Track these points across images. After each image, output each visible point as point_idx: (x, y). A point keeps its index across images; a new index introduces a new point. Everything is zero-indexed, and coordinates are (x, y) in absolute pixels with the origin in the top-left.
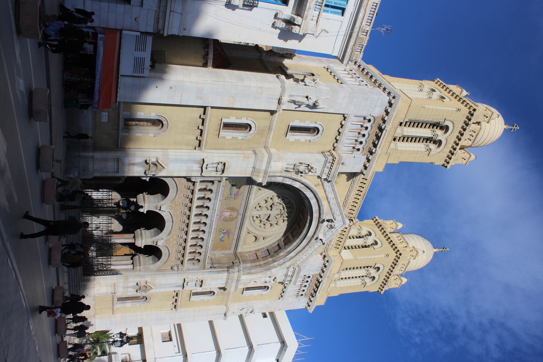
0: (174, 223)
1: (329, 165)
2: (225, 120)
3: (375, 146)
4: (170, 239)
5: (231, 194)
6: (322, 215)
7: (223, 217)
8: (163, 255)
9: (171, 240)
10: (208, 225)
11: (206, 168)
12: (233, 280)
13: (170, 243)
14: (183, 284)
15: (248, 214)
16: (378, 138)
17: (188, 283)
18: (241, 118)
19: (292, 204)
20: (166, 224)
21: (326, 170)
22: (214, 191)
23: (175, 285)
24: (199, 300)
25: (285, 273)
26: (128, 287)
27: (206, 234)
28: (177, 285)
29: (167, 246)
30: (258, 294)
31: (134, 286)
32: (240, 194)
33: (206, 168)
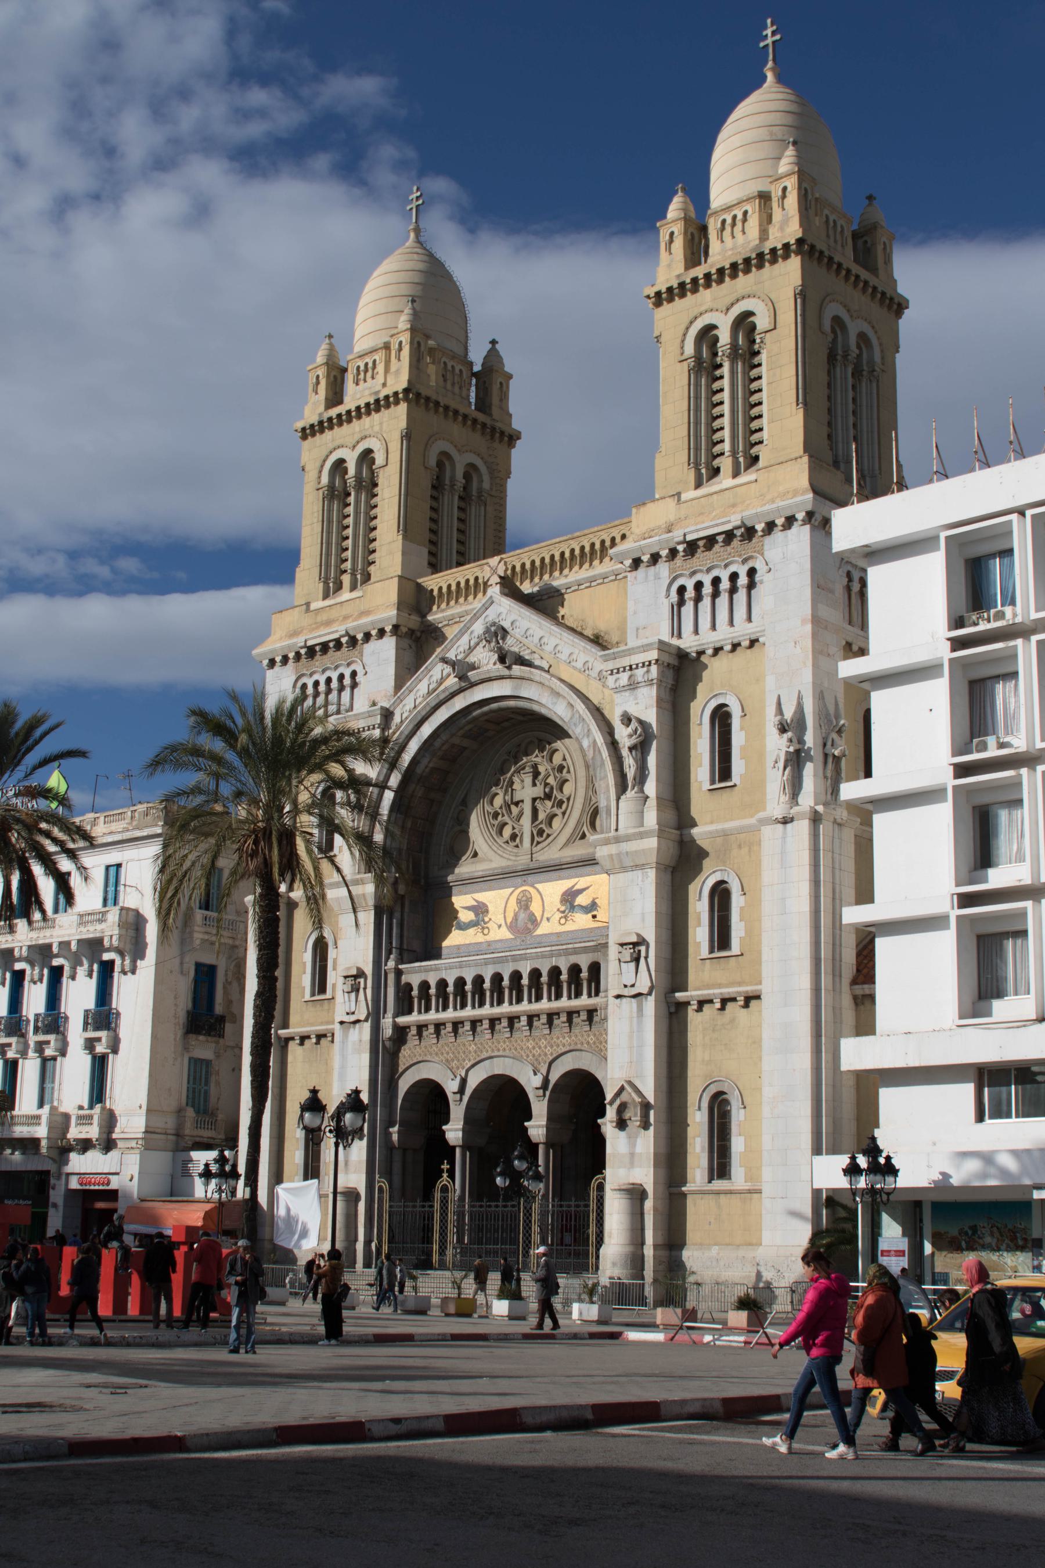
0: (496, 1053)
4: (534, 1056)
6: (451, 691)
7: (530, 926)
8: (576, 1066)
9: (537, 1051)
10: (498, 968)
11: (353, 1013)
12: (619, 855)
13: (546, 1055)
14: (635, 996)
16: (325, 647)
17: (625, 986)
18: (304, 964)
20: (497, 1072)
23: (635, 1020)
24: (743, 923)
25: (627, 694)
26: (632, 1155)
28: (635, 1015)
29: (551, 1058)
30: (742, 729)
31: (629, 1137)
32: (476, 901)
33: (353, 1013)
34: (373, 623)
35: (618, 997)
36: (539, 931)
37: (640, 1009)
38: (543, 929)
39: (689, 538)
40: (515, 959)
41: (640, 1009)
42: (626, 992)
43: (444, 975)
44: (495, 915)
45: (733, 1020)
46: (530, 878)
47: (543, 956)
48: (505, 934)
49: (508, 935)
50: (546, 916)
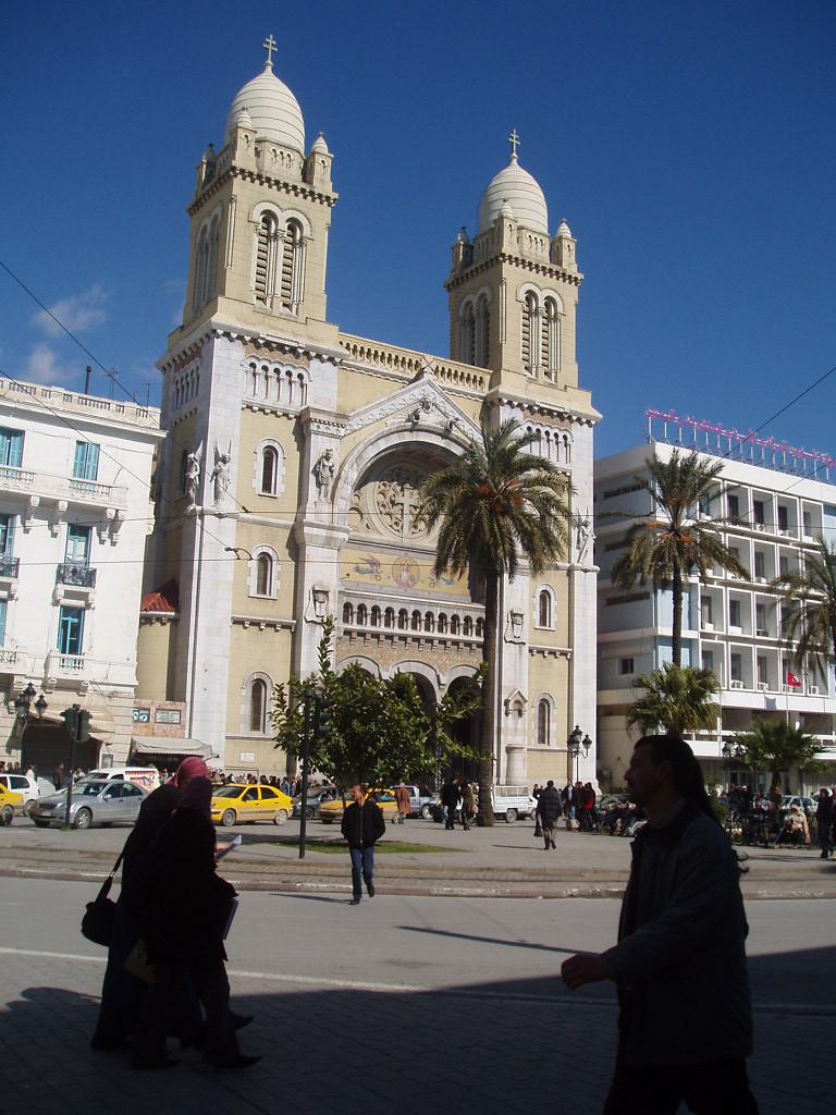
1: (323, 428)
2: (253, 592)
3: (293, 350)
5: (372, 572)
10: (418, 608)
15: (406, 542)
19: (393, 471)
21: (333, 430)
22: (361, 601)
26: (516, 729)
27: (433, 610)
34: (317, 348)
35: (511, 642)
36: (417, 587)
37: (521, 651)
38: (419, 586)
39: (542, 405)
40: (431, 604)
41: (521, 651)
42: (516, 640)
43: (378, 604)
44: (386, 570)
45: (551, 663)
46: (410, 554)
47: (449, 607)
48: (392, 582)
49: (395, 584)
50: (421, 578)
